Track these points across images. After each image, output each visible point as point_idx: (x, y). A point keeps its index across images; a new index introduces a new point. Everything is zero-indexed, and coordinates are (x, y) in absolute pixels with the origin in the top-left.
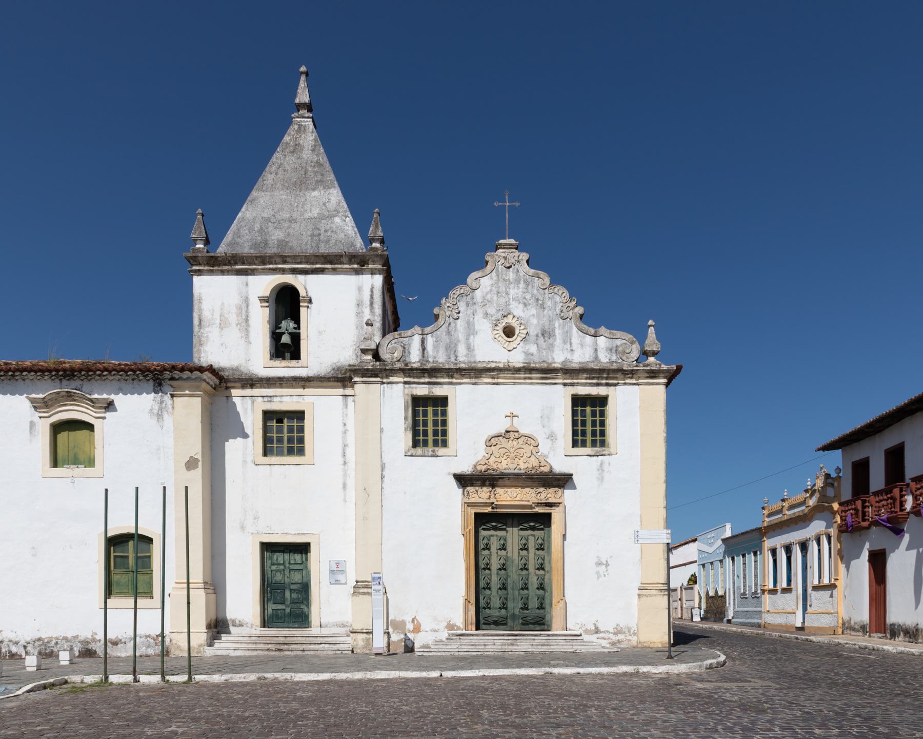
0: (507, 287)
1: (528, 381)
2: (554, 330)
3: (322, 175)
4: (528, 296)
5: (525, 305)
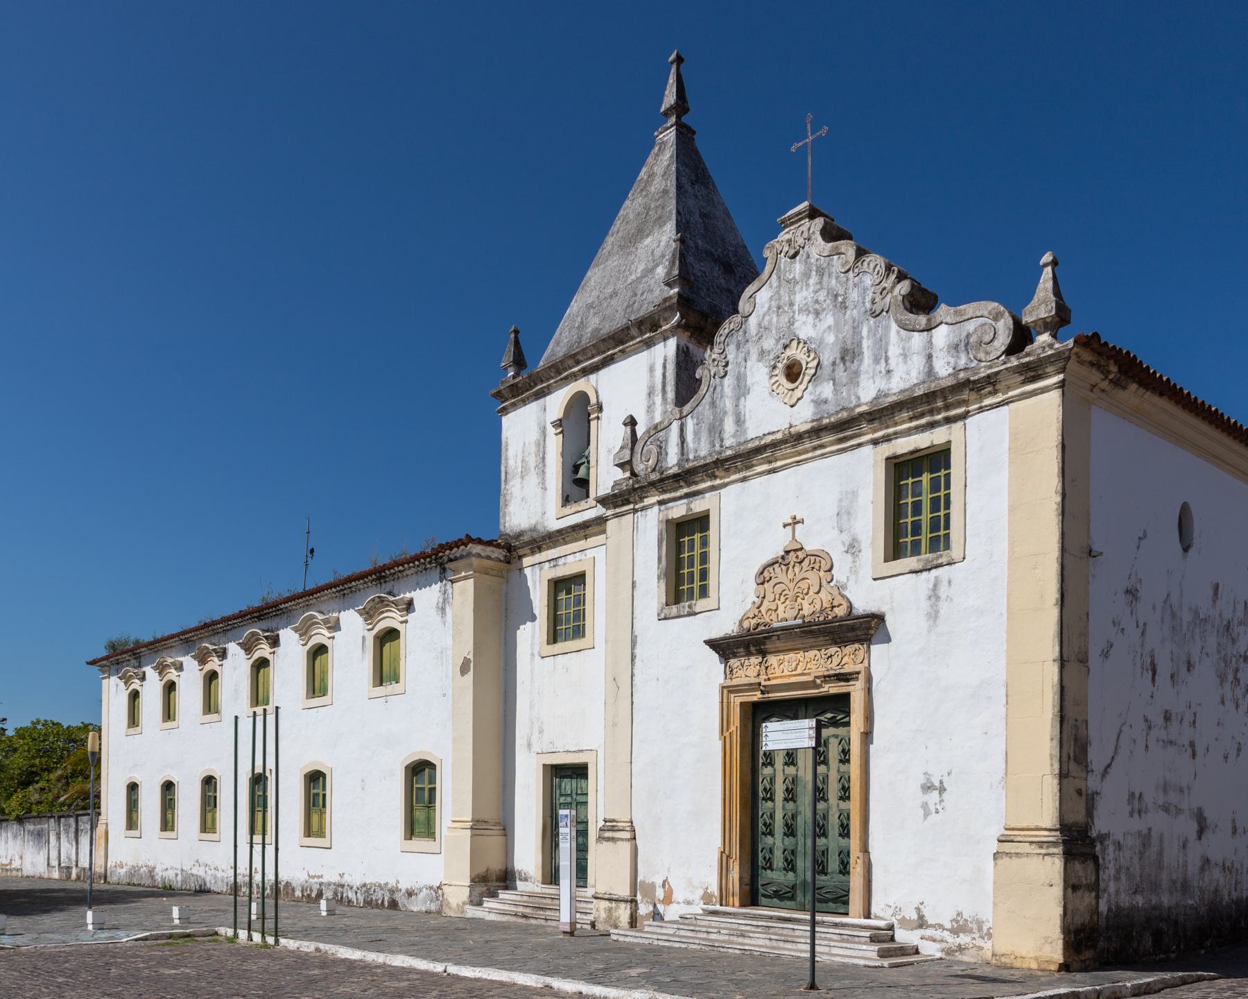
0: (792, 292)
1: (819, 452)
2: (860, 344)
4: (822, 296)
5: (817, 313)
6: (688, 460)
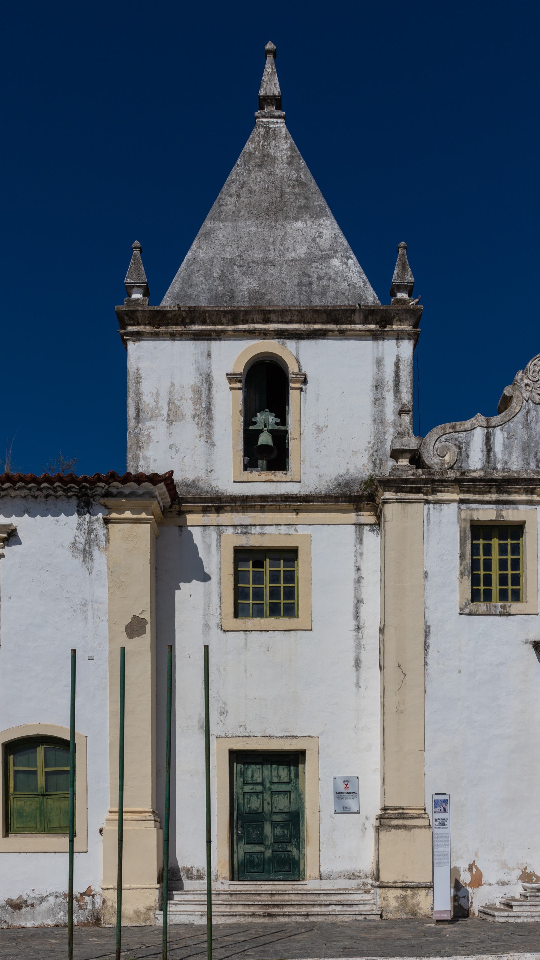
3: (306, 198)
6: (495, 469)
